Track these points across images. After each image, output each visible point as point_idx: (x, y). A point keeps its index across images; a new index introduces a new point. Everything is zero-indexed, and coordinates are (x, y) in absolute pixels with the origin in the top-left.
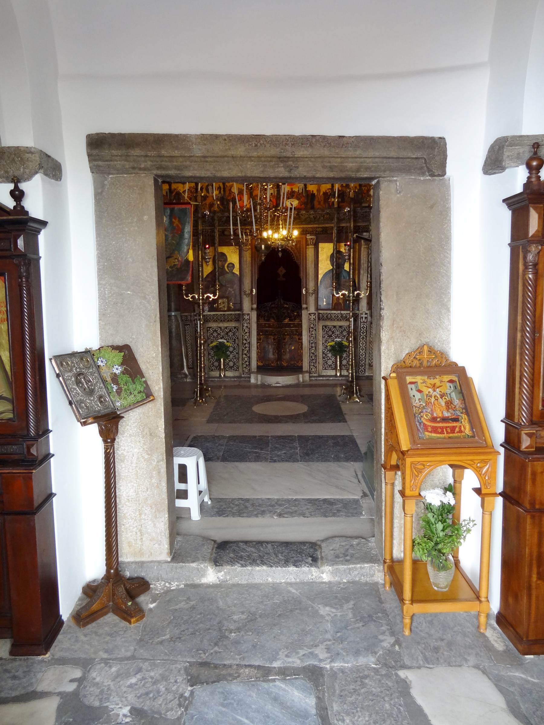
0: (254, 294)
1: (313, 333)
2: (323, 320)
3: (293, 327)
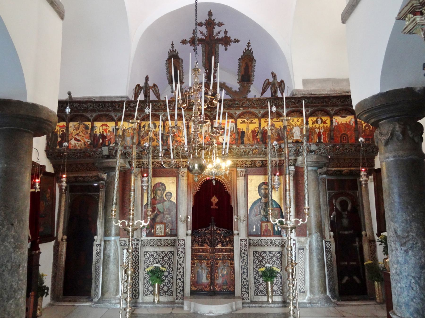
0: (189, 220)
1: (245, 258)
2: (254, 245)
3: (225, 252)
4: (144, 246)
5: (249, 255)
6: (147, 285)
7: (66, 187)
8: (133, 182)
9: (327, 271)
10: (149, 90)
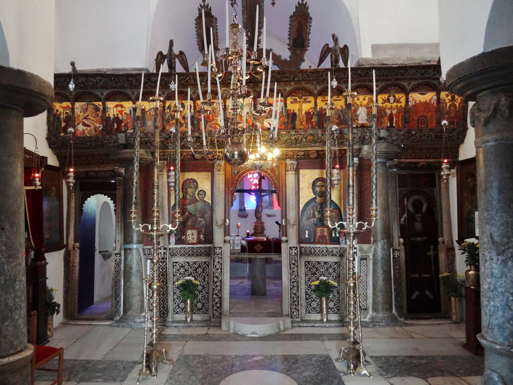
1: (295, 270)
2: (306, 255)
4: (172, 255)
5: (300, 266)
6: (178, 301)
7: (75, 184)
8: (156, 177)
9: (394, 285)
10: (174, 59)
